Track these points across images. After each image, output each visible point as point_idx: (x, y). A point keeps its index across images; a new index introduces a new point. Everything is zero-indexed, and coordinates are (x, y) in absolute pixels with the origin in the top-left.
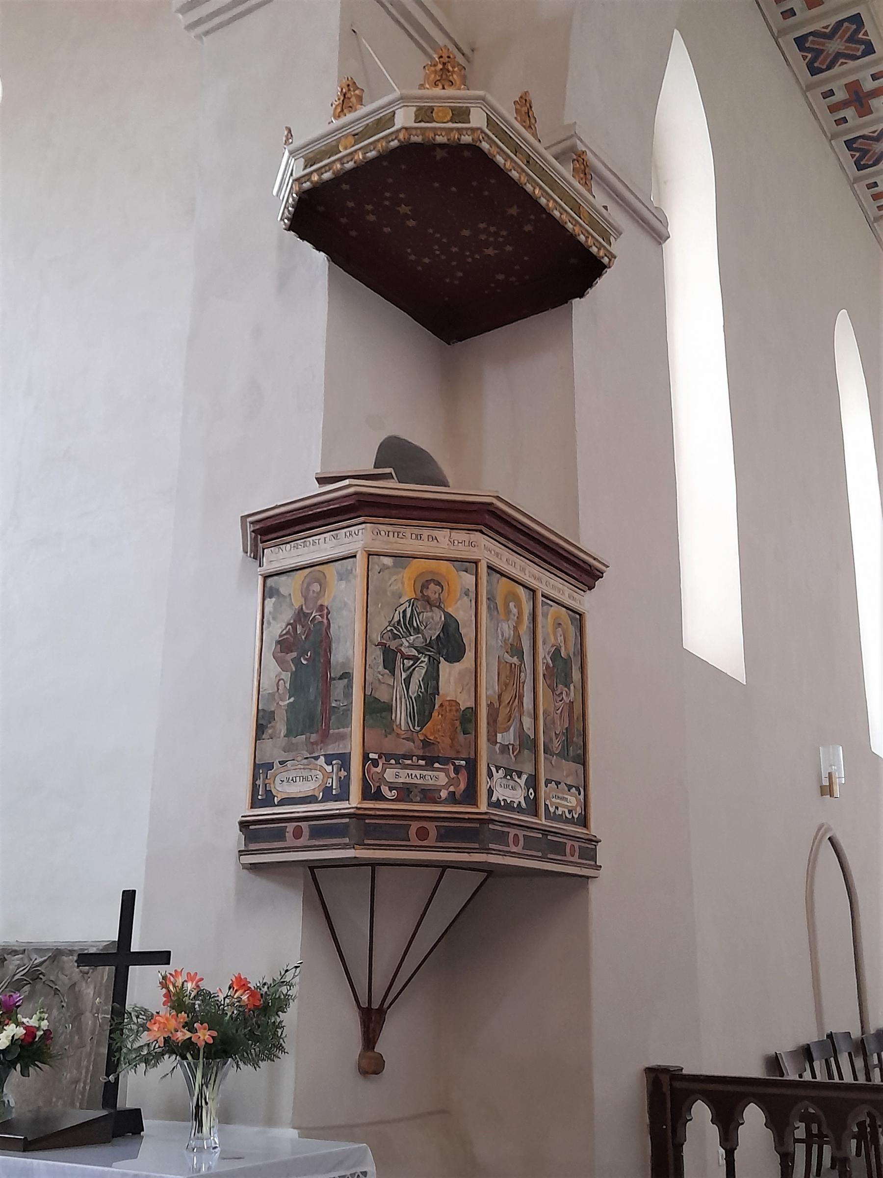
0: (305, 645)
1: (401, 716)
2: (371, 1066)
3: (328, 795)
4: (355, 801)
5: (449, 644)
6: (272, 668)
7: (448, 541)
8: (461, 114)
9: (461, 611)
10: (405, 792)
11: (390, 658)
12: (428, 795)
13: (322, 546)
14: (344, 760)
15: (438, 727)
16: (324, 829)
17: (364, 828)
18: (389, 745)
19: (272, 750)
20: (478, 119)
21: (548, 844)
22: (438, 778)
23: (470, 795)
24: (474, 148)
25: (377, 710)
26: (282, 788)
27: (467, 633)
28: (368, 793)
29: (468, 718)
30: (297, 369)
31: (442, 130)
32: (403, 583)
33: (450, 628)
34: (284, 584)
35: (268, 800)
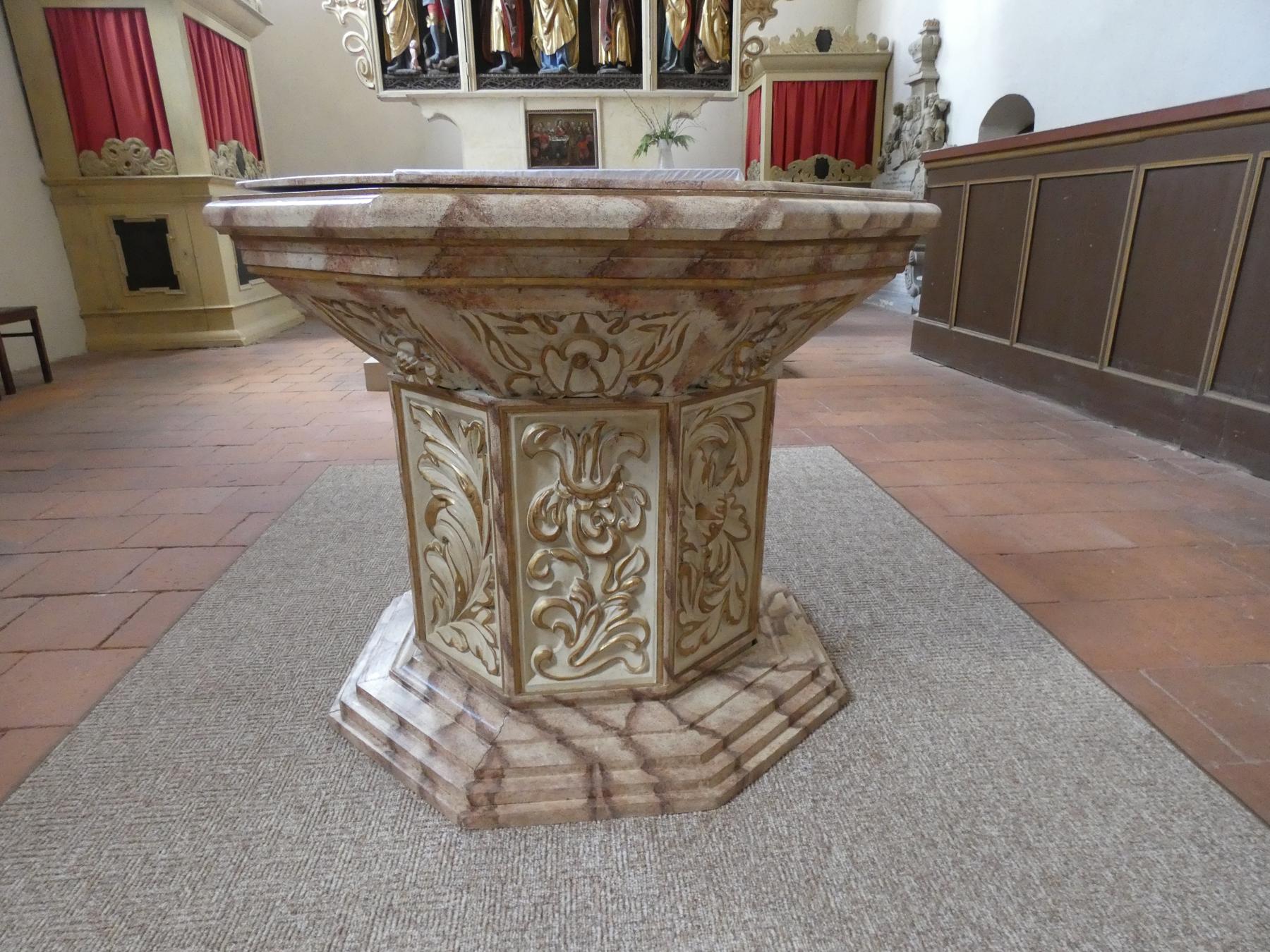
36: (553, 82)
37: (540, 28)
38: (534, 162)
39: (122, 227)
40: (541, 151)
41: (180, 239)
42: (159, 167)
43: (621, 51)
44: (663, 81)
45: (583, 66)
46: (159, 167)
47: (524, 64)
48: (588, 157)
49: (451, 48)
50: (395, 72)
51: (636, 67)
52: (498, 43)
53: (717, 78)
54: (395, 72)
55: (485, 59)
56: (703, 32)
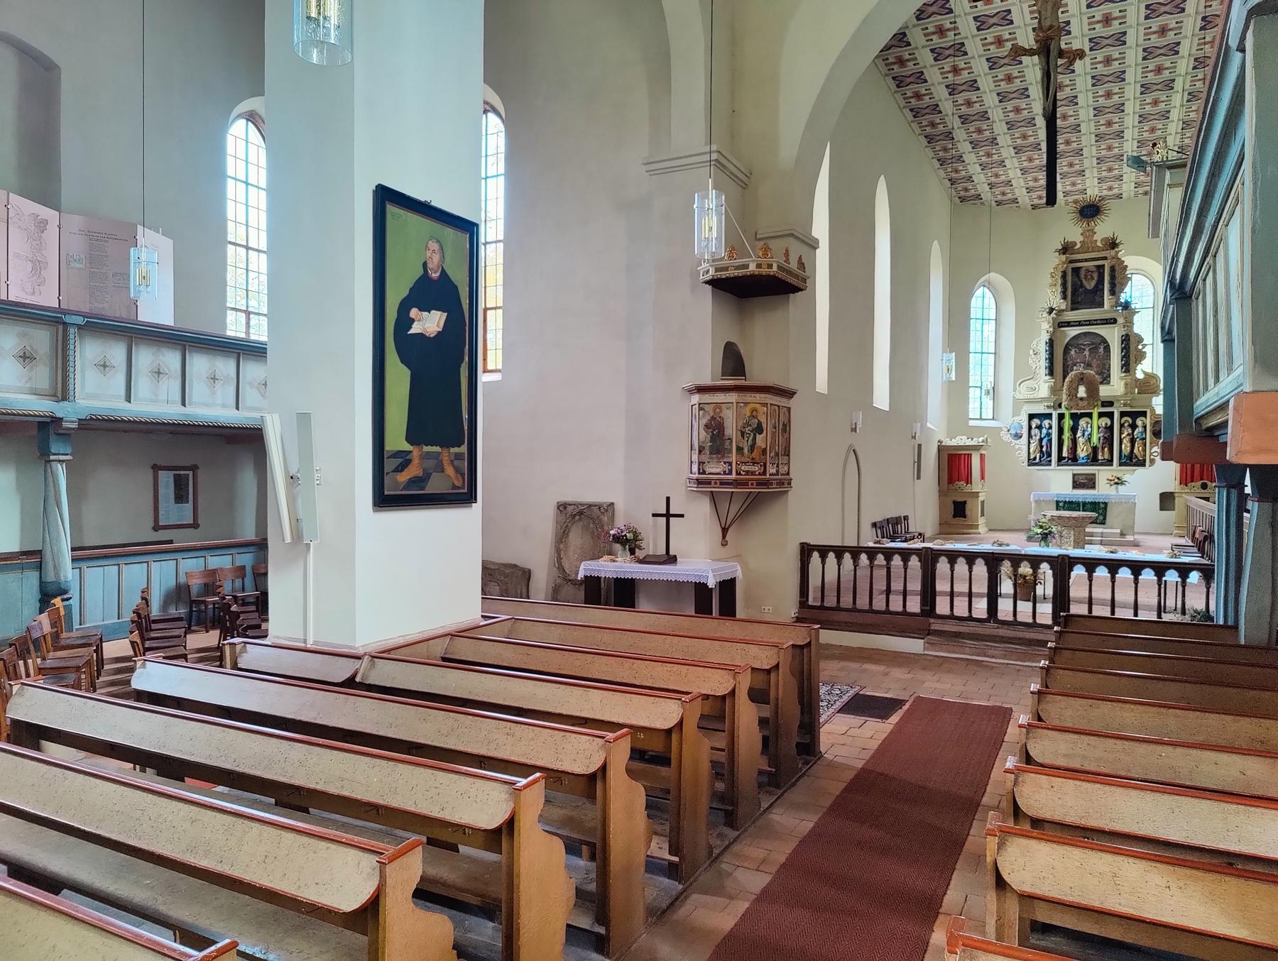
0: (715, 428)
1: (746, 451)
2: (724, 544)
3: (725, 473)
4: (734, 476)
5: (759, 429)
6: (703, 433)
7: (759, 397)
8: (770, 266)
9: (763, 420)
10: (747, 473)
11: (743, 434)
12: (753, 473)
13: (720, 398)
14: (730, 464)
15: (756, 454)
16: (723, 483)
17: (736, 483)
18: (743, 459)
19: (705, 458)
20: (775, 268)
21: (781, 483)
22: (755, 468)
23: (764, 473)
24: (774, 276)
25: (740, 449)
26: (708, 470)
27: (764, 426)
28: (738, 474)
29: (764, 451)
30: (700, 328)
31: (764, 271)
32: (747, 411)
33: (760, 424)
34: (706, 407)
35: (704, 473)
36: (1083, 465)
37: (1079, 450)
38: (1074, 487)
39: (954, 502)
40: (1077, 485)
41: (968, 506)
42: (968, 489)
43: (1106, 456)
44: (1121, 464)
45: (1093, 459)
46: (968, 489)
47: (1074, 459)
48: (1093, 487)
49: (1049, 455)
50: (1031, 462)
51: (1111, 460)
52: (1065, 454)
53: (1142, 463)
54: (1031, 462)
55: (1060, 458)
56: (1136, 451)
